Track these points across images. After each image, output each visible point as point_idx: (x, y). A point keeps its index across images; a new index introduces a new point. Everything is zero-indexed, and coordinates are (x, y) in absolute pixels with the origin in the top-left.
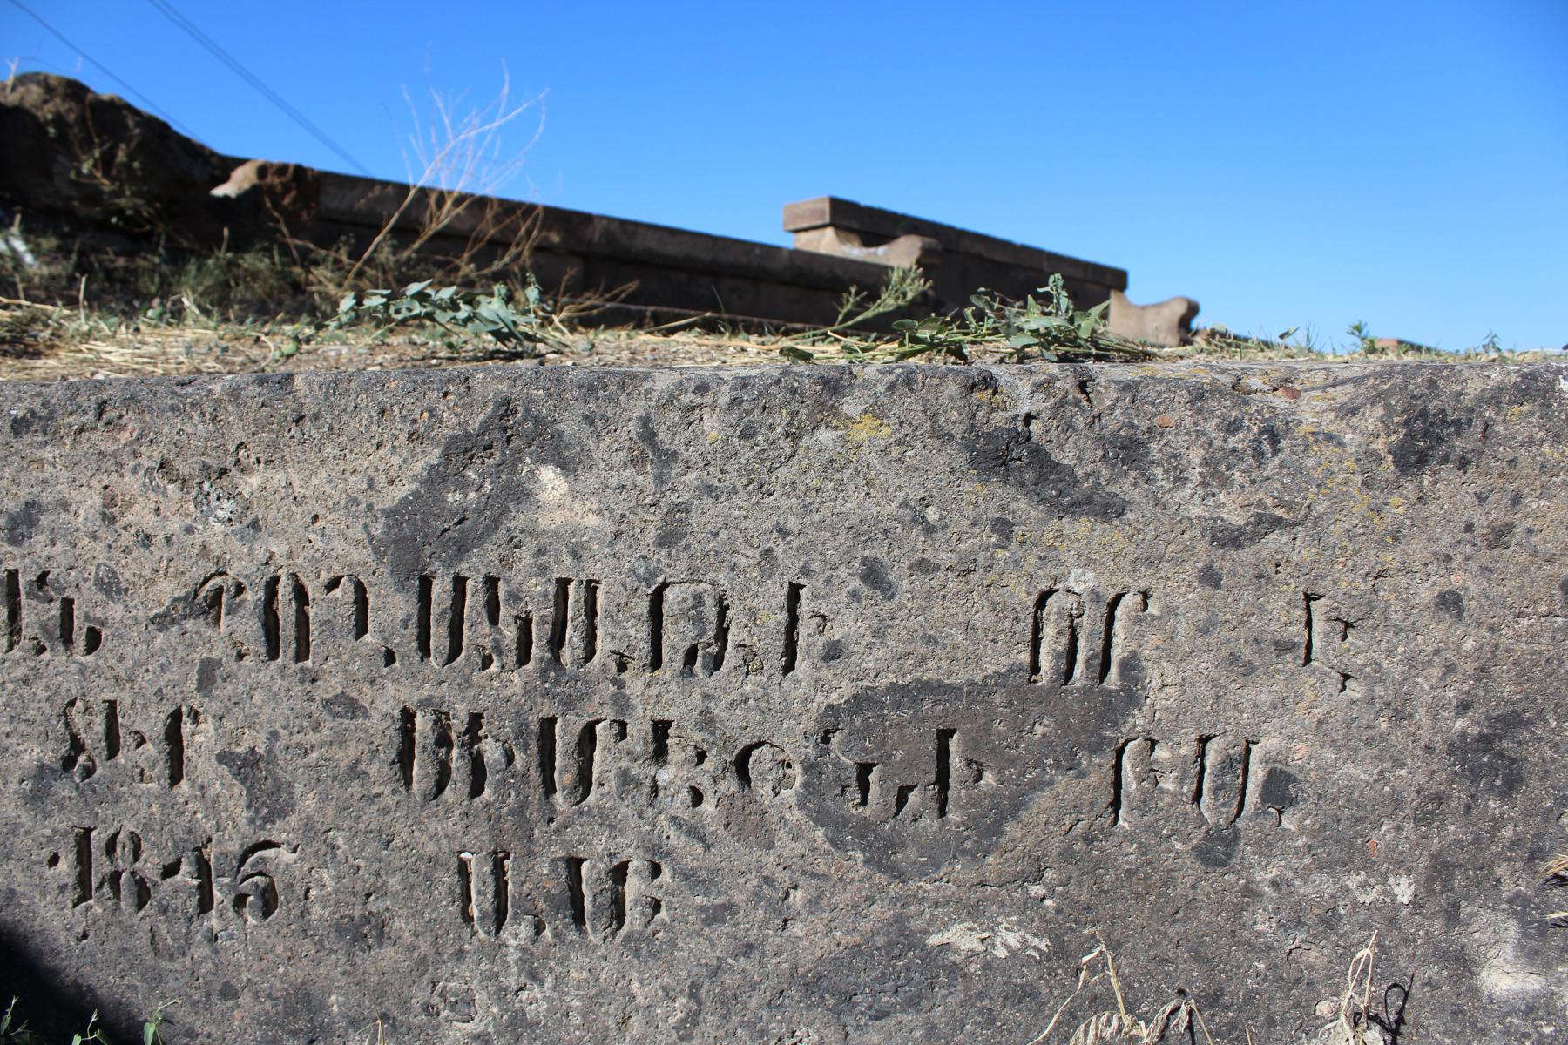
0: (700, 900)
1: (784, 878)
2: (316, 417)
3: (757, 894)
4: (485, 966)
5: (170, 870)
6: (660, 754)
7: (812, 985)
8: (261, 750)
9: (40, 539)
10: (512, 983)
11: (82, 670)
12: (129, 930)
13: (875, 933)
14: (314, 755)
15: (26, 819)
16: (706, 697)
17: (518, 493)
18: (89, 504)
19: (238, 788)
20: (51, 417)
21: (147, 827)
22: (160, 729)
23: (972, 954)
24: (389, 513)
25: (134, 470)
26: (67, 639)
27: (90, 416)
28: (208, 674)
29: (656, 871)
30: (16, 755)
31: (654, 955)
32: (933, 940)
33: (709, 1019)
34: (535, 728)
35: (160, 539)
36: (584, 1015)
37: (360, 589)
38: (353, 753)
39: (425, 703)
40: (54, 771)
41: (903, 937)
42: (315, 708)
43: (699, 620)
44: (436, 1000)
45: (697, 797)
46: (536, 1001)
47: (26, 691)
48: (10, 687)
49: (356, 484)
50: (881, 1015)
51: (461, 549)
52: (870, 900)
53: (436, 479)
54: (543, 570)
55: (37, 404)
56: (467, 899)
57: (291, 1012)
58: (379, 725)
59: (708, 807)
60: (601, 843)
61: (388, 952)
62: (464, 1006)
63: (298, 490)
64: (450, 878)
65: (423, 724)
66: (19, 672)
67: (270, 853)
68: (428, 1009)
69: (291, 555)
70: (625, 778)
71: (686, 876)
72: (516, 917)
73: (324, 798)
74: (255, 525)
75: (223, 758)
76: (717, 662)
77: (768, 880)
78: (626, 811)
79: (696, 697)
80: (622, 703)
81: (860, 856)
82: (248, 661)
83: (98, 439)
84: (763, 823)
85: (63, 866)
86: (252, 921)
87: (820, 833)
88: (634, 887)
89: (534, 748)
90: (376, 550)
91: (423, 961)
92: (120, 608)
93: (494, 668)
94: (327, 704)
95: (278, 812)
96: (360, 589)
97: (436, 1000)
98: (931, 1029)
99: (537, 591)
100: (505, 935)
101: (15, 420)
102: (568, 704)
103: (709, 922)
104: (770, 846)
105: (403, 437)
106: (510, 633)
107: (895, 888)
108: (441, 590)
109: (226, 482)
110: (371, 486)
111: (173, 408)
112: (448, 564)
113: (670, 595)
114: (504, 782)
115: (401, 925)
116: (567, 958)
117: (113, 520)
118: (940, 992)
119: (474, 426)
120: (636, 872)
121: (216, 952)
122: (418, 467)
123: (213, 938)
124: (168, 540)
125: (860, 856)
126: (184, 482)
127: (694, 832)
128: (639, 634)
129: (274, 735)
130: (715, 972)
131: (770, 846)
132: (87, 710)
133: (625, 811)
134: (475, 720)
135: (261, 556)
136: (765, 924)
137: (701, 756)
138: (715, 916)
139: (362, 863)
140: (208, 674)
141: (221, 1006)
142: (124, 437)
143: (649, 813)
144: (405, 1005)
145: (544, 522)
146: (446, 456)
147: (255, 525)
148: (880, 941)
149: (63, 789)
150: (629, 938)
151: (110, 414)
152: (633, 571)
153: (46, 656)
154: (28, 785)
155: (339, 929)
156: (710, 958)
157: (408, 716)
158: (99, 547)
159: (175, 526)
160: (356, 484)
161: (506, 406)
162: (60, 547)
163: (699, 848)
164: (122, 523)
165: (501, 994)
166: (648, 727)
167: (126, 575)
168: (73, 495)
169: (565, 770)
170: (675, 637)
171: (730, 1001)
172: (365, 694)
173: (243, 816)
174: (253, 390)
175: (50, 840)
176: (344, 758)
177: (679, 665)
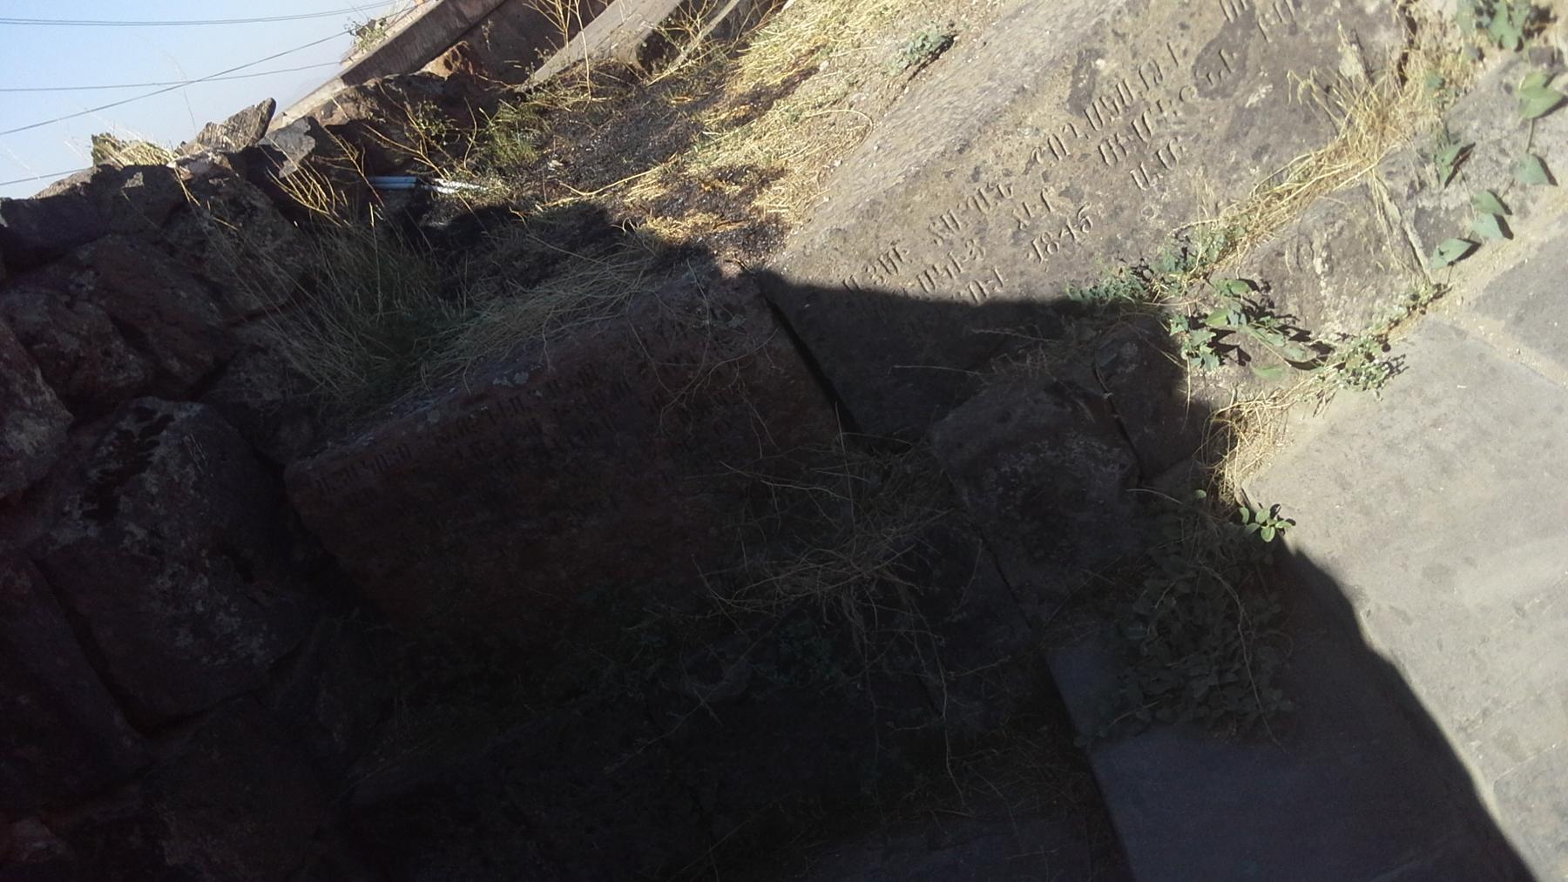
0: (1191, 138)
1: (1206, 118)
2: (1037, 91)
3: (1203, 127)
4: (1150, 197)
5: (1060, 235)
6: (1161, 111)
7: (1227, 140)
8: (1068, 185)
9: (983, 176)
10: (1159, 196)
11: (1012, 200)
12: (1058, 258)
13: (1233, 114)
14: (1082, 176)
15: (1016, 250)
16: (1165, 87)
17: (1094, 73)
18: (990, 157)
19: (1068, 200)
20: (968, 142)
21: (1049, 227)
22: (1040, 200)
23: (1257, 102)
24: (1068, 101)
25: (998, 139)
26: (1002, 195)
27: (979, 135)
28: (1045, 177)
29: (1176, 139)
30: (1006, 235)
31: (1188, 161)
32: (1247, 105)
33: (1209, 167)
34: (1131, 126)
35: (1015, 151)
36: (1179, 190)
37: (1070, 125)
38: (1092, 167)
39: (1102, 142)
40: (1017, 232)
41: (1240, 109)
42: (1077, 163)
43: (1152, 70)
44: (1143, 216)
45: (1175, 113)
46: (1166, 197)
47: (999, 217)
48: (995, 219)
49: (1056, 100)
50: (1246, 134)
51: (1090, 96)
52: (1228, 107)
53: (1074, 84)
54: (1111, 86)
55: (962, 142)
56: (1136, 183)
57: (1109, 247)
58: (1095, 156)
59: (1179, 114)
60: (1161, 142)
61: (1126, 213)
62: (1150, 212)
63: (1042, 113)
64: (1131, 181)
65: (1102, 148)
66: (995, 213)
67: (1082, 211)
68: (1141, 220)
69: (1050, 130)
70: (1158, 122)
71: (1185, 135)
72: (1152, 178)
73: (1090, 184)
74: (1037, 129)
75: (1060, 195)
76: (1161, 77)
77: (1203, 121)
78: (1162, 130)
79: (1163, 89)
80: (1148, 104)
81: (1219, 98)
82: (1054, 165)
83: (984, 138)
84: (1194, 108)
85: (1031, 255)
86: (1087, 232)
87: (1208, 100)
88: (1173, 149)
89: (1133, 131)
90: (1071, 113)
91: (1135, 208)
92: (1013, 177)
93: (1113, 119)
94: (1079, 160)
95: (1082, 197)
96: (1070, 125)
97: (1143, 216)
98: (1259, 129)
99: (1112, 91)
100: (1151, 185)
101: (958, 150)
102: (1135, 114)
103: (1196, 142)
104: (1198, 112)
105: (1061, 80)
106: (1113, 108)
107: (1231, 100)
108: (1089, 111)
109: (1023, 125)
110: (1060, 97)
111: (1000, 116)
112: (1089, 103)
113: (1143, 69)
114: (1132, 146)
115: (1125, 203)
116: (1168, 179)
117: (999, 156)
118: (1256, 117)
119: (1076, 63)
120: (1173, 143)
121: (1082, 247)
122: (1068, 84)
123: (1079, 244)
124: (1017, 150)
125: (1219, 98)
126: (1012, 133)
127: (1180, 122)
128: (1141, 84)
129: (1070, 178)
130: (1204, 154)
131: (1198, 112)
132: (1018, 209)
133: (1162, 130)
134: (1115, 136)
135: (1042, 136)
136: (1209, 132)
137: (1170, 102)
138: (1196, 140)
139: (1107, 194)
140: (1045, 177)
141: (1090, 261)
142: (989, 133)
143: (1168, 126)
144: (1136, 223)
145: (1105, 74)
146: (1073, 76)
147: (1037, 129)
148: (1236, 115)
149: (1023, 235)
150: (1180, 161)
151: (982, 131)
152: (1132, 70)
153: (999, 204)
154: (1012, 241)
155: (1111, 216)
156: (1201, 151)
157: (1099, 148)
158: (1000, 167)
159: (1017, 146)
160: (1056, 100)
161: (1080, 54)
162: (989, 173)
163: (1183, 126)
164: (1002, 155)
165: (1158, 202)
166: (1156, 105)
167: (1010, 168)
168: (985, 158)
169: (1142, 132)
170: (1149, 80)
171: (1211, 160)
172: (1087, 151)
173: (1072, 206)
174: (1017, 96)
175: (1025, 251)
176: (1090, 171)
177: (1154, 84)
